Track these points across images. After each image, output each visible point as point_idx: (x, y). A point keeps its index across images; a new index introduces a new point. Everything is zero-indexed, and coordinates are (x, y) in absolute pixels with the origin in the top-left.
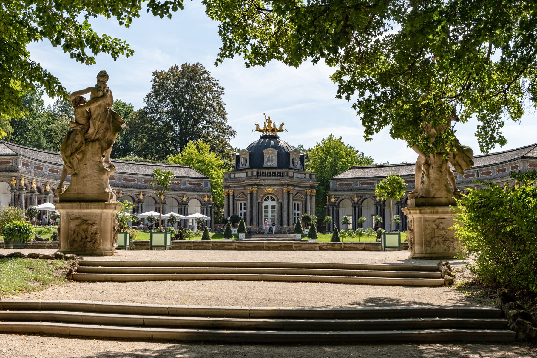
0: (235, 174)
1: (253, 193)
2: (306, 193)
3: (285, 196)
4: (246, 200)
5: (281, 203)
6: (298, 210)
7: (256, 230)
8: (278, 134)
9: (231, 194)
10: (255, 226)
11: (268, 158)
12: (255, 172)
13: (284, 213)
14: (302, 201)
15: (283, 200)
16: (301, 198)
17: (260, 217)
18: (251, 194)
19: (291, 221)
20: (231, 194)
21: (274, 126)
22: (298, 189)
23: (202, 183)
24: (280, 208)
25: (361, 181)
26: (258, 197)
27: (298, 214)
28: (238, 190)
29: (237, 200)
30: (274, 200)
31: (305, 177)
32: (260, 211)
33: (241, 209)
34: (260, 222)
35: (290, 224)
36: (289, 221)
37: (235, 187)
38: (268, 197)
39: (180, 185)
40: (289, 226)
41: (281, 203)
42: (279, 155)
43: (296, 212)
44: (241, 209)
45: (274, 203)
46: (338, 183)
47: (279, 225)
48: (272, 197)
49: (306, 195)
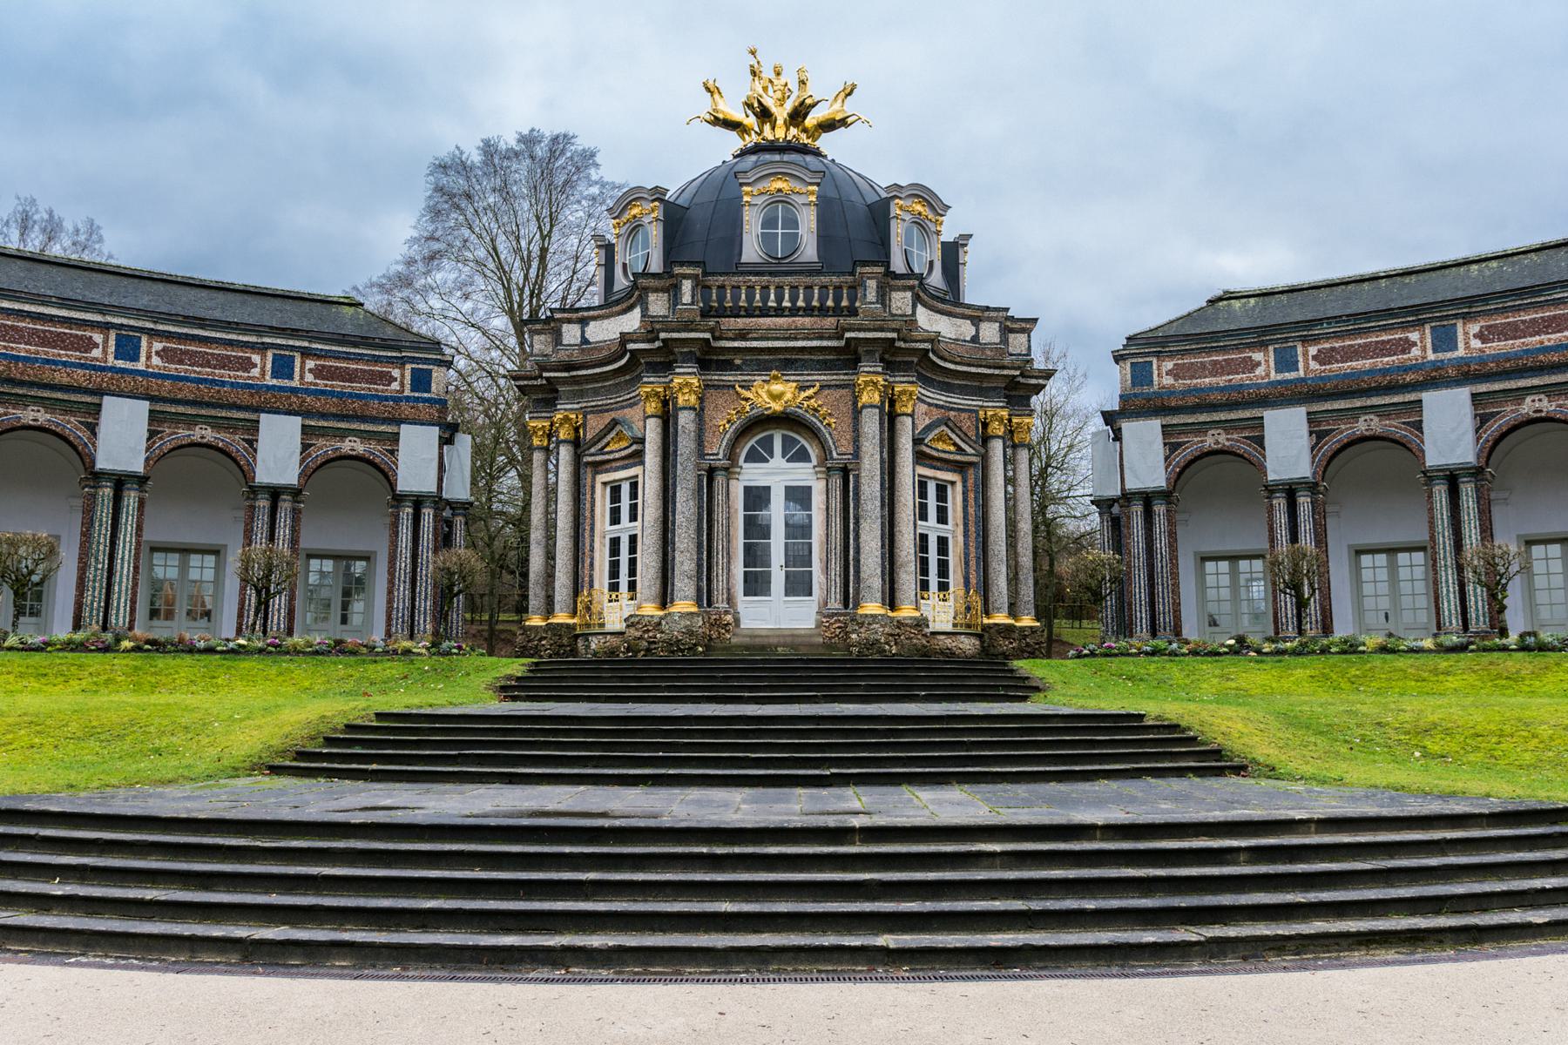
0: (584, 322)
1: (677, 409)
2: (985, 425)
3: (871, 425)
4: (637, 457)
5: (845, 471)
6: (942, 518)
7: (691, 633)
8: (827, 143)
9: (563, 434)
10: (683, 605)
11: (769, 223)
12: (687, 286)
13: (864, 525)
14: (960, 467)
15: (857, 454)
16: (960, 450)
17: (720, 559)
18: (667, 419)
19: (907, 579)
20: (563, 434)
21: (802, 82)
22: (941, 398)
23: (396, 373)
24: (836, 503)
25: (1315, 340)
26: (708, 436)
27: (943, 543)
28: (600, 410)
29: (598, 467)
30: (802, 456)
31: (975, 339)
32: (720, 516)
33: (615, 519)
34: (719, 585)
35: (899, 595)
36: (892, 582)
37: (581, 394)
38: (767, 444)
39: (255, 372)
40: (893, 607)
41: (845, 471)
42: (828, 210)
43: (931, 527)
44: (615, 519)
45: (804, 474)
46: (1169, 365)
47: (835, 604)
48: (788, 443)
49: (986, 440)
